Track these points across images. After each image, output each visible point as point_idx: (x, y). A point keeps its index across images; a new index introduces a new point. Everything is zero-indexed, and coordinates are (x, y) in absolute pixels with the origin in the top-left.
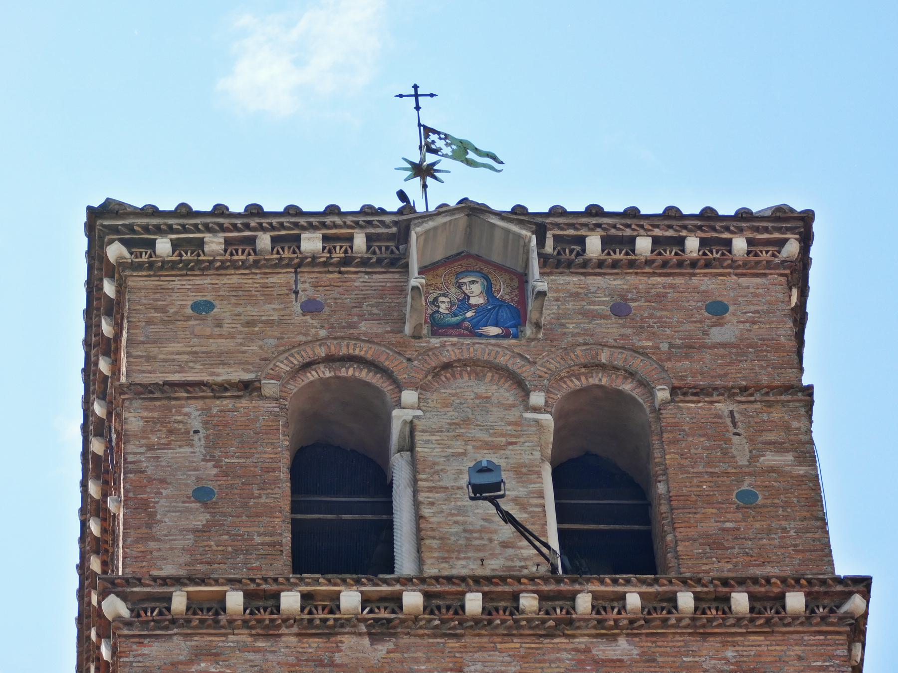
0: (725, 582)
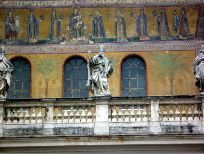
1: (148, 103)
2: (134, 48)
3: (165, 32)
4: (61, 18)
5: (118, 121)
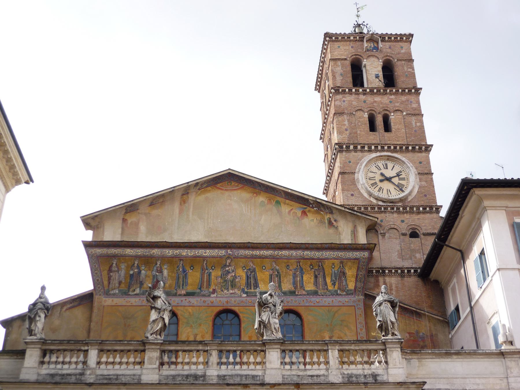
0: (405, 88)
1: (325, 348)
2: (290, 302)
3: (322, 286)
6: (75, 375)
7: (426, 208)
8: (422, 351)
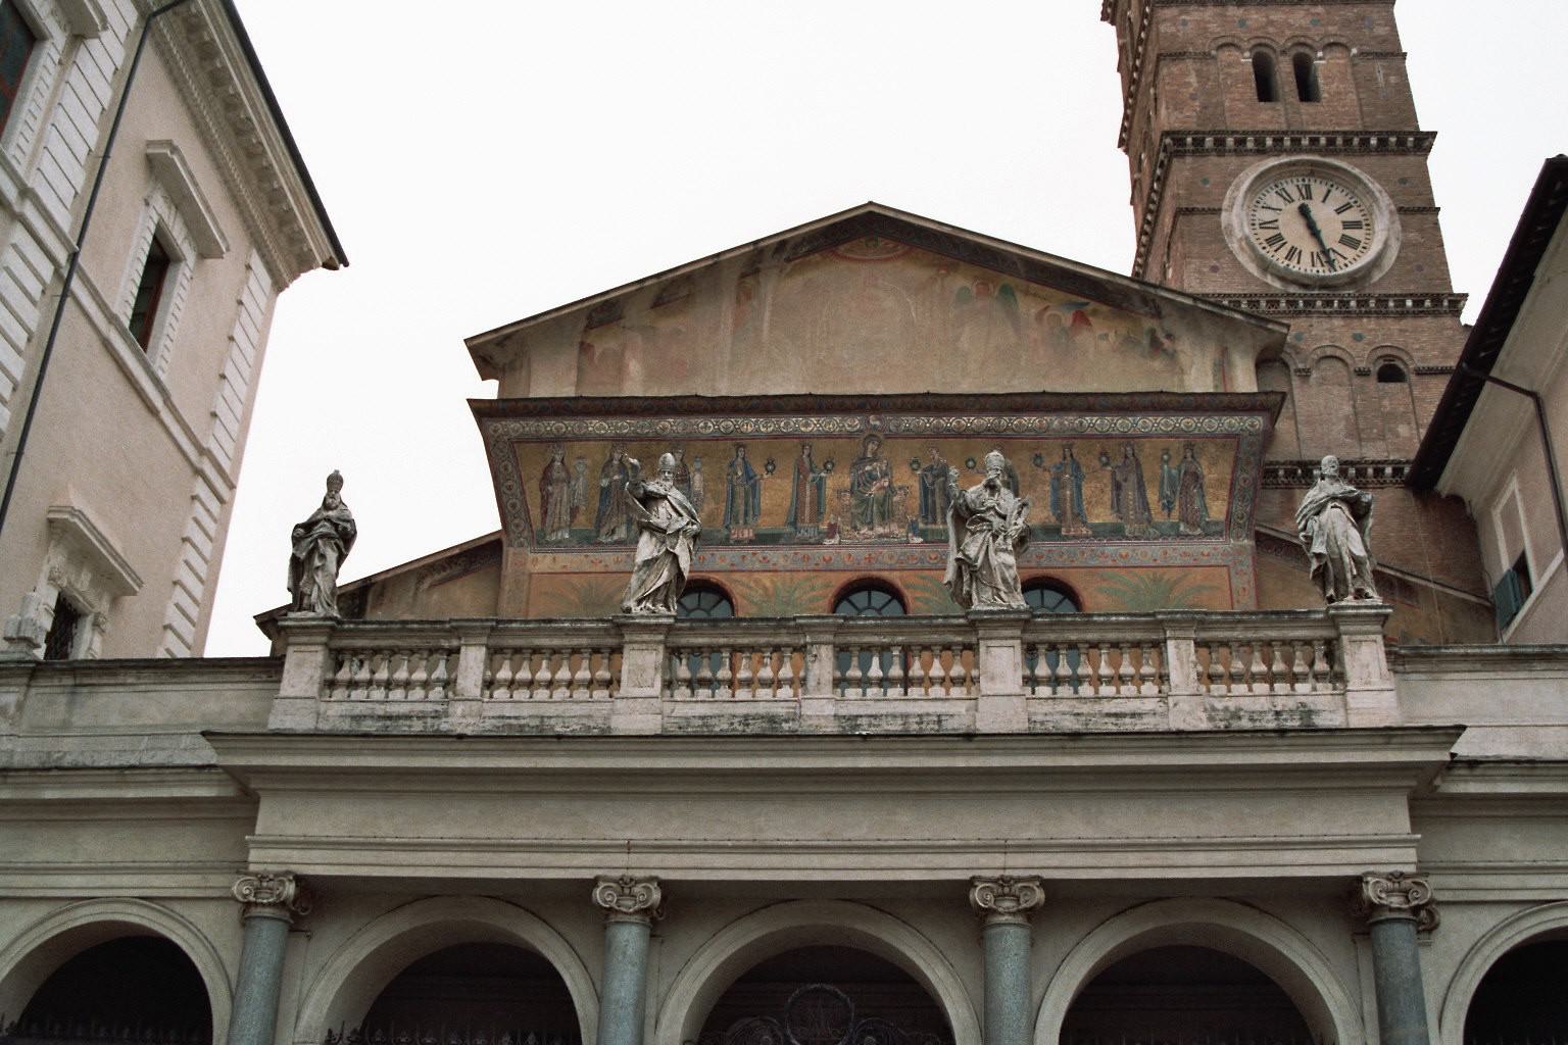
4: (825, 466)
5: (1058, 695)
6: (421, 717)
7: (1423, 302)
8: (1443, 651)
